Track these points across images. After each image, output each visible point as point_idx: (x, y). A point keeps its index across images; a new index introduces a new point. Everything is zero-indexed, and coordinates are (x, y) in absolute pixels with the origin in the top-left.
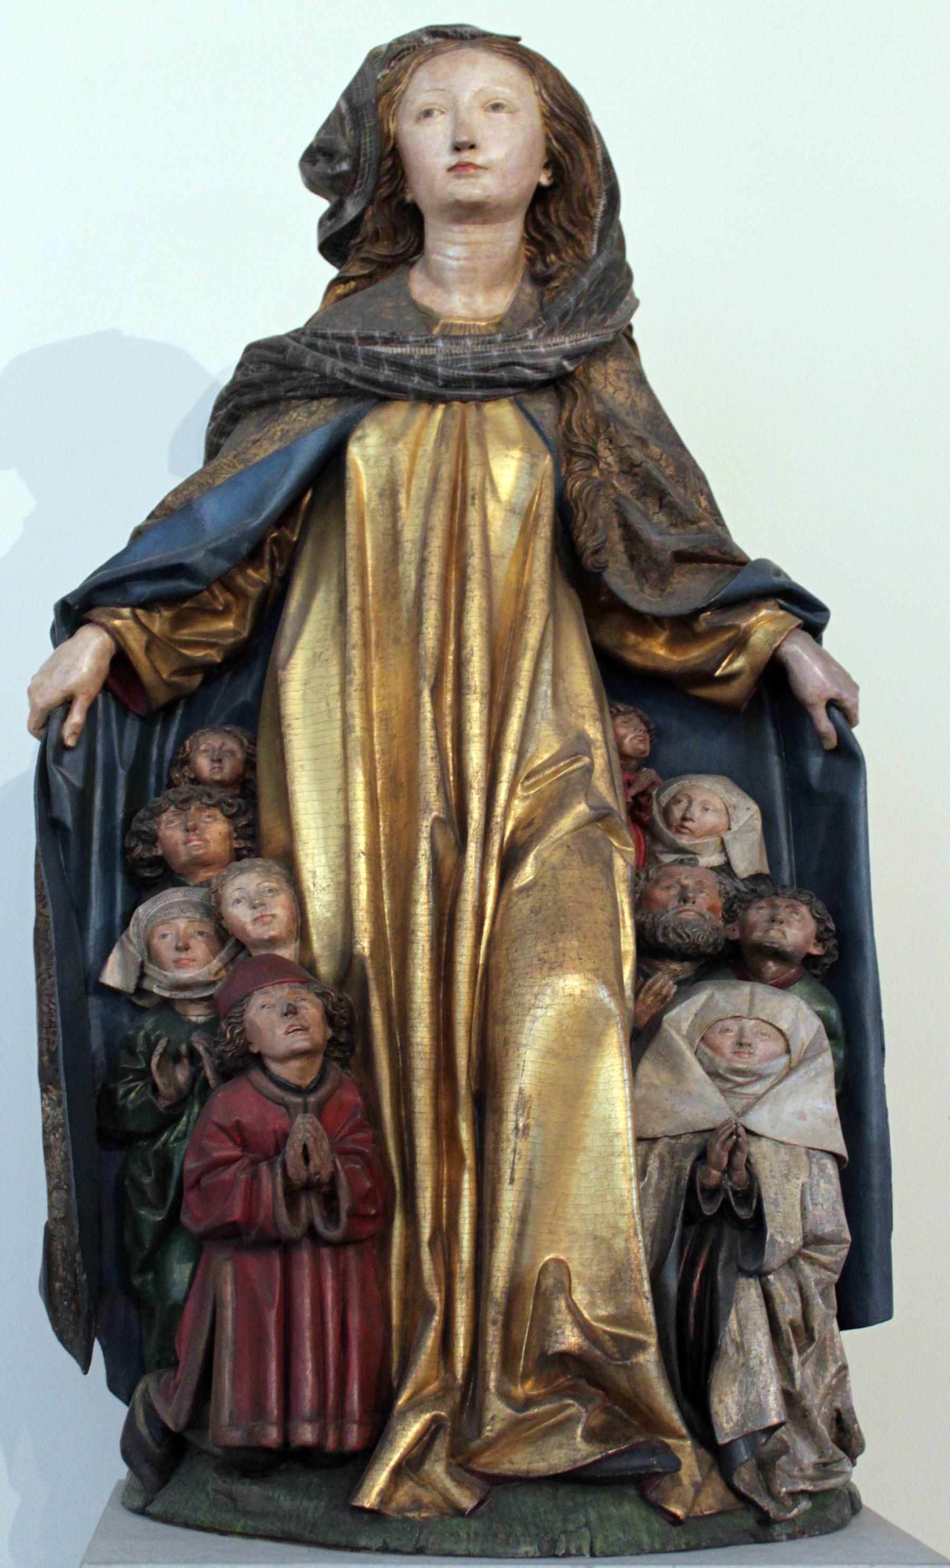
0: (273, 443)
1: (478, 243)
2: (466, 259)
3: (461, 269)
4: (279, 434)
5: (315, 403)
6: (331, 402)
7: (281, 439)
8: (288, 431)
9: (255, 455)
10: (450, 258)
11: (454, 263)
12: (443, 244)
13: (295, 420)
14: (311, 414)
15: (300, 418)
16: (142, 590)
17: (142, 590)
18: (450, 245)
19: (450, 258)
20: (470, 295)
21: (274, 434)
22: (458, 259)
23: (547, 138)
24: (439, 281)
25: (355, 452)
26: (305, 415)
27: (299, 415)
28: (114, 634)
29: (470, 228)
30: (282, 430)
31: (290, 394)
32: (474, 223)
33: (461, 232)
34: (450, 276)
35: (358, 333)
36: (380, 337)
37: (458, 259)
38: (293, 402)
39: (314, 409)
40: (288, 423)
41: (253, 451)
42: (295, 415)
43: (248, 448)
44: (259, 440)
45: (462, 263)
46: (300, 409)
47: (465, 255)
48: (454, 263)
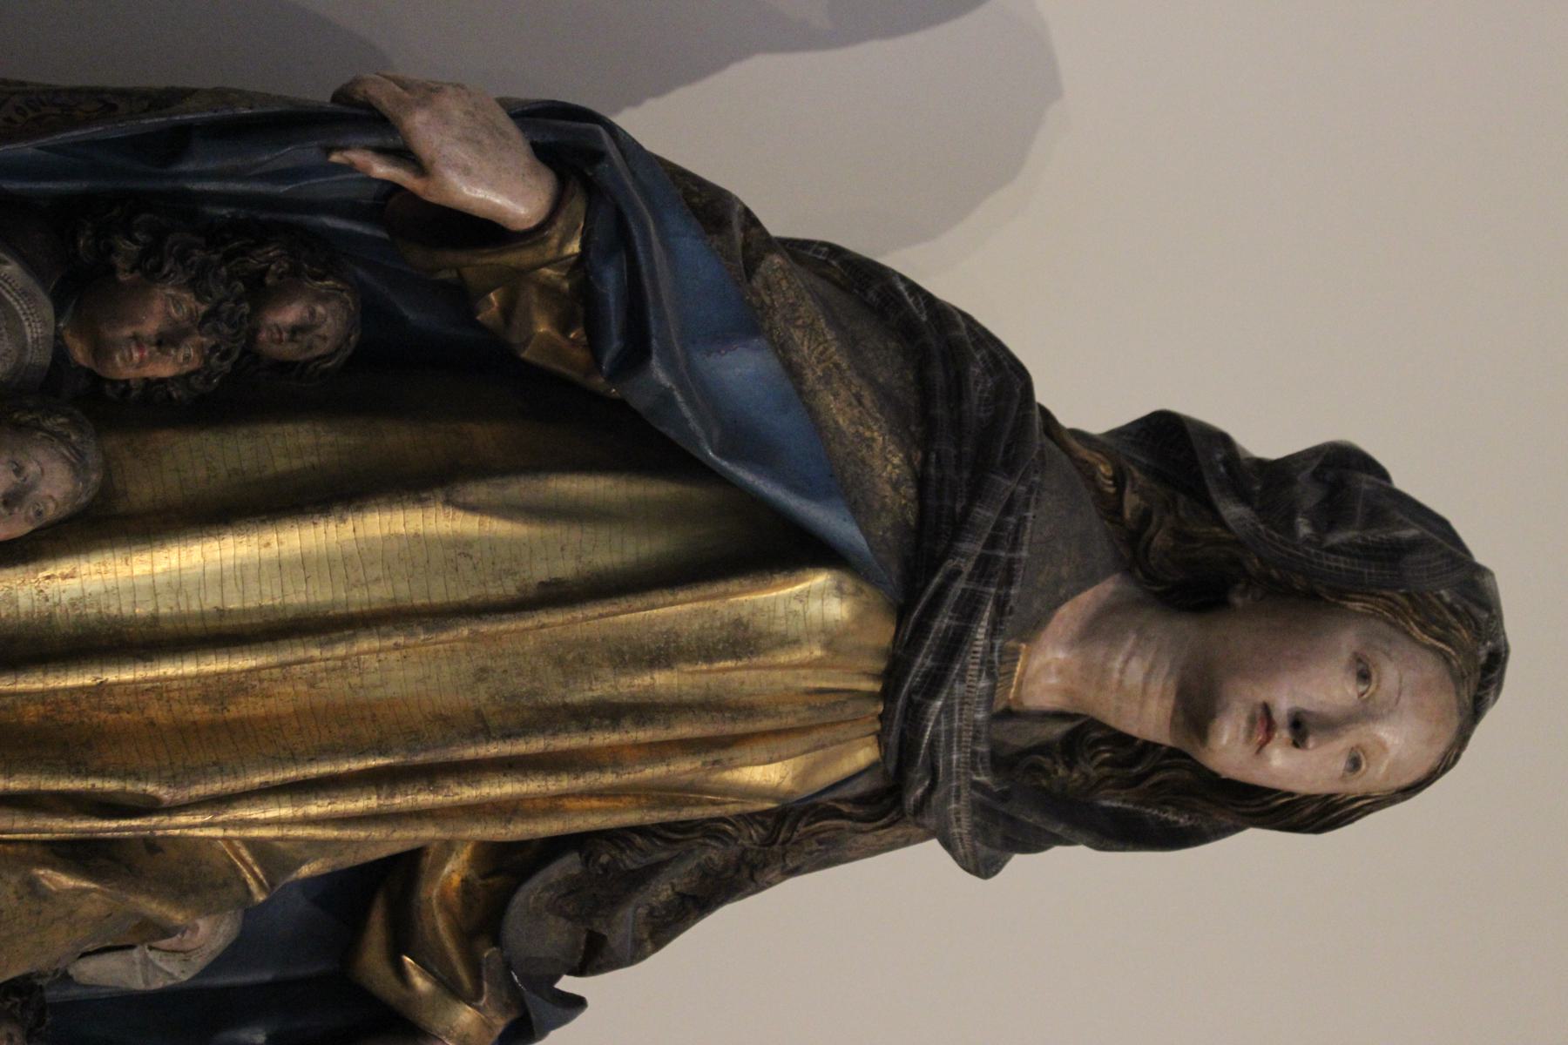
0: (852, 423)
1: (1142, 705)
2: (1120, 682)
3: (1105, 671)
4: (868, 434)
5: (912, 492)
6: (911, 517)
7: (858, 434)
8: (869, 447)
9: (836, 395)
10: (1126, 662)
11: (1117, 664)
12: (1150, 657)
13: (887, 459)
14: (896, 486)
15: (889, 468)
16: (610, 281)
17: (610, 281)
18: (1147, 665)
19: (1126, 662)
20: (1060, 672)
21: (869, 428)
22: (1122, 672)
23: (1291, 794)
24: (1093, 630)
25: (821, 579)
26: (894, 476)
27: (895, 467)
28: (536, 234)
29: (1169, 703)
30: (873, 440)
31: (933, 456)
32: (1175, 711)
33: (1164, 689)
34: (1099, 652)
35: (1020, 560)
36: (1007, 595)
37: (1122, 672)
38: (920, 454)
39: (903, 489)
40: (884, 448)
41: (843, 393)
42: (896, 461)
43: (848, 386)
44: (860, 403)
45: (1116, 675)
46: (905, 468)
47: (1128, 682)
48: (1117, 664)
